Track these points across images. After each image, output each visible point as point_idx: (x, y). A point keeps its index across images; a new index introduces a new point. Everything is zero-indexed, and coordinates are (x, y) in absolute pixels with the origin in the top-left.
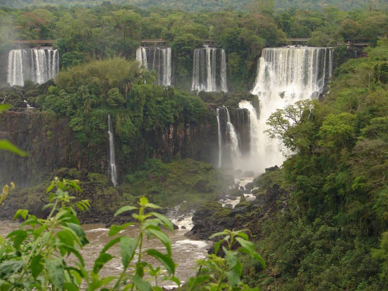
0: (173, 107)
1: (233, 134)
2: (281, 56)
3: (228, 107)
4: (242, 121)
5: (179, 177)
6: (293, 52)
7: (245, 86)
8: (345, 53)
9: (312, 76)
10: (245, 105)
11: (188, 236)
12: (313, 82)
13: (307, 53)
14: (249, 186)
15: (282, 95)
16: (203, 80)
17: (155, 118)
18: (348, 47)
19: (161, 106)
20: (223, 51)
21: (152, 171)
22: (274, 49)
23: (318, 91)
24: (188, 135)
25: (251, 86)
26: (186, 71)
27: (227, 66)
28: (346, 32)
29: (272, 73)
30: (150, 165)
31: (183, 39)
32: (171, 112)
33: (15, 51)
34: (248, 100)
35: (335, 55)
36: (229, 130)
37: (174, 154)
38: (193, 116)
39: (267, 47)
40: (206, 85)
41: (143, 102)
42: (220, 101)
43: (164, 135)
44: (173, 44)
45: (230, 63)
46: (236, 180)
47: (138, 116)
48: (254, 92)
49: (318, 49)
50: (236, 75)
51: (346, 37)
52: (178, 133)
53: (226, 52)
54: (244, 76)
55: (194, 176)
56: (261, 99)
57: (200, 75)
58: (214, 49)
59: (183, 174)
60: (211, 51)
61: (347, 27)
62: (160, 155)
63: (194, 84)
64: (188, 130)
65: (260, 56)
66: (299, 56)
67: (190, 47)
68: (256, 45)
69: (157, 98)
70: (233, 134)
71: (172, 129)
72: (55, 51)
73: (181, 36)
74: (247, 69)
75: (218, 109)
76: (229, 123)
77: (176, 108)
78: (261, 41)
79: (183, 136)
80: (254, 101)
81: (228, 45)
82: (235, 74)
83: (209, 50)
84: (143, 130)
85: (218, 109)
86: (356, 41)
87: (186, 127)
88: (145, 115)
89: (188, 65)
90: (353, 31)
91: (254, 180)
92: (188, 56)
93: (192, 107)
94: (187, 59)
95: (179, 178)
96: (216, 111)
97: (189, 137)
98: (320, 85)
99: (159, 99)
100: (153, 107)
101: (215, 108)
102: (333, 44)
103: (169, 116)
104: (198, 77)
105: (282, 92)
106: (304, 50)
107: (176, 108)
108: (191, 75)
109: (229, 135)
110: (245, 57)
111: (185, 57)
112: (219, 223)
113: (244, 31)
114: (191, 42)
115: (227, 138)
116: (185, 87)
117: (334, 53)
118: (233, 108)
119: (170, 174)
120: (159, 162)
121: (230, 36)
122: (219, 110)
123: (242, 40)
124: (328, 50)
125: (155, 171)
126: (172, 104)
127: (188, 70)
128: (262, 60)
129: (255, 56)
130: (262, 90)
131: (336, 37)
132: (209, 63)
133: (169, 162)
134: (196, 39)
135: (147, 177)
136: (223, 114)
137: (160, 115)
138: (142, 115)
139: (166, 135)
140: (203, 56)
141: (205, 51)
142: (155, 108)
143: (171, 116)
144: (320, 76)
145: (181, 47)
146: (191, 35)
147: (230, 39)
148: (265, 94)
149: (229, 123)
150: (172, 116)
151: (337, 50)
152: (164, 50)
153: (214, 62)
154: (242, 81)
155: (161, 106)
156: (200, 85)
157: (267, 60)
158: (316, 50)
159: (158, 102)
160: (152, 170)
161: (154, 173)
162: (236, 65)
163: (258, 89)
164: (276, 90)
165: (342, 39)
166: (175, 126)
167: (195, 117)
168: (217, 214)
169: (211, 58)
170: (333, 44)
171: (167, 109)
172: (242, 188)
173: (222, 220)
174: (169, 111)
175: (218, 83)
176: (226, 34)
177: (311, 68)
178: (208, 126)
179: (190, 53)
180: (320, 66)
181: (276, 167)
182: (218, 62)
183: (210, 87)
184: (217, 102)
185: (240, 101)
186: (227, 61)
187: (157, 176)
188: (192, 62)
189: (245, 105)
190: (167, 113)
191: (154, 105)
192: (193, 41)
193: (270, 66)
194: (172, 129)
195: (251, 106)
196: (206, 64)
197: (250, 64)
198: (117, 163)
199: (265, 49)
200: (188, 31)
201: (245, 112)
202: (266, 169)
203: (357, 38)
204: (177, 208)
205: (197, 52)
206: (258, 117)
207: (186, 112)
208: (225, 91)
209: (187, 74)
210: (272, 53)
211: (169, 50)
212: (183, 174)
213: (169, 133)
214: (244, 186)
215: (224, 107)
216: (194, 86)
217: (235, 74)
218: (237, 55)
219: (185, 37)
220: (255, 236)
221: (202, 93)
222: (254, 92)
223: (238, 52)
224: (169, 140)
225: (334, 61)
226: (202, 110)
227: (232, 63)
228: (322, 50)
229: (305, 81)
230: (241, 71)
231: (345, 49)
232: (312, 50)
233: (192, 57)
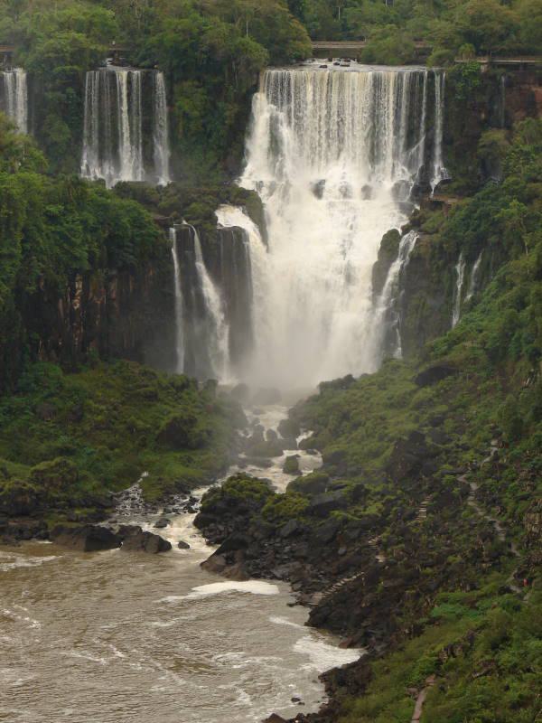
0: (85, 229)
1: (210, 290)
2: (310, 88)
3: (195, 222)
5: (115, 409)
6: (341, 78)
7: (219, 166)
8: (477, 82)
9: (389, 138)
10: (231, 217)
11: (214, 568)
12: (395, 155)
13: (377, 83)
14: (290, 429)
15: (318, 191)
16: (109, 151)
17: (45, 258)
18: (483, 68)
19: (59, 228)
20: (160, 76)
21: (46, 397)
22: (293, 73)
23: (407, 177)
24: (114, 300)
25: (238, 169)
26: (66, 128)
27: (171, 117)
28: (478, 29)
29: (286, 132)
30: (37, 381)
31: (59, 47)
32: (83, 243)
34: (235, 204)
35: (449, 89)
36: (197, 282)
37: (84, 350)
38: (126, 252)
39: (273, 64)
40: (117, 164)
41: (22, 219)
42: (172, 207)
43: (61, 301)
44: (30, 59)
45: (180, 108)
47: (11, 256)
48: (246, 182)
49: (407, 71)
50: (194, 139)
51: (477, 39)
52: (91, 294)
53: (170, 80)
54: (217, 139)
55: (150, 406)
56: (270, 203)
57: (101, 137)
58: (136, 72)
59: (123, 403)
60: (129, 76)
61: (478, 18)
62: (53, 353)
63: (85, 161)
64: (113, 286)
65: (255, 89)
66: (353, 87)
67: (75, 67)
68: (249, 63)
69: (47, 208)
70: (210, 290)
71: (79, 285)
73: (50, 37)
74: (224, 124)
75: (173, 230)
76: (200, 265)
77: (94, 230)
78: (262, 53)
79: (102, 303)
80: (248, 201)
81: (175, 62)
82: (192, 135)
83: (123, 74)
84: (18, 291)
85: (173, 230)
86: (502, 53)
87: (110, 279)
88: (24, 251)
89: (72, 112)
90: (497, 27)
91: (292, 413)
92: (70, 90)
93: (127, 227)
94: (68, 98)
95: (115, 413)
96: (168, 235)
97: (116, 304)
98: (410, 164)
99: (53, 209)
100: (40, 230)
101: (166, 226)
102: (440, 61)
103: (78, 252)
104: (95, 142)
105: (315, 177)
106: (370, 73)
107: (94, 230)
108: (78, 138)
109: (200, 299)
110: (217, 91)
111: (63, 93)
112: (285, 532)
113: (217, 30)
114: (78, 55)
115: (197, 305)
116: (64, 169)
117: (446, 82)
118: (208, 226)
119: (91, 402)
120: (56, 370)
121: (181, 39)
122: (177, 233)
123: (212, 48)
124: (431, 75)
125: (51, 395)
126: (84, 222)
127: (71, 126)
129: (244, 90)
130: (266, 178)
131: (447, 43)
132: (125, 108)
133: (77, 371)
134: (93, 47)
135: (34, 411)
136: (184, 240)
137: (57, 250)
138: (18, 252)
139: (65, 302)
140: (107, 90)
141: (113, 76)
142: (47, 235)
143: (82, 252)
144: (409, 145)
145: (52, 67)
146: (81, 37)
147: (184, 46)
148: (272, 189)
149: (200, 265)
150: (86, 254)
151: (456, 76)
152: (8, 76)
153: (137, 103)
154: (211, 154)
155: (59, 228)
156: (101, 165)
157: (274, 101)
158: (400, 76)
159: (52, 219)
160: (46, 393)
161: (50, 399)
162: (196, 113)
163: (253, 174)
164: (301, 179)
165: (467, 47)
166: (86, 278)
167: (132, 254)
168: (271, 510)
169: (129, 95)
170: (440, 61)
171: (74, 236)
172: (271, 433)
173: (291, 525)
174: (79, 241)
175: (149, 161)
176: (171, 36)
177: (389, 121)
178: (151, 273)
179: (76, 81)
180: (412, 117)
181: (349, 378)
182: (148, 106)
184: (163, 211)
185: (217, 207)
186: (170, 103)
187: (60, 410)
188: (80, 105)
189: (231, 217)
190: (73, 245)
191: (44, 226)
192: (82, 51)
193: (282, 116)
194: (79, 285)
195: (247, 219)
196: (115, 111)
197: (230, 110)
199: (268, 71)
200: (64, 26)
201: (238, 234)
202: (324, 386)
203: (506, 45)
204: (134, 491)
205: (92, 80)
207: (114, 242)
209: (69, 136)
210: (285, 84)
211: (21, 75)
212: (123, 403)
213: (73, 297)
214: (274, 428)
215: (184, 222)
216: (87, 166)
217: (192, 135)
218: (197, 87)
219: (64, 39)
220: (429, 570)
221: (123, 189)
222: (246, 182)
223: (198, 79)
224: (72, 314)
225: (446, 100)
226: (150, 235)
227: (186, 108)
228: (415, 74)
229: (374, 155)
230: (209, 127)
231: (475, 74)
232: (389, 73)
233: (80, 94)
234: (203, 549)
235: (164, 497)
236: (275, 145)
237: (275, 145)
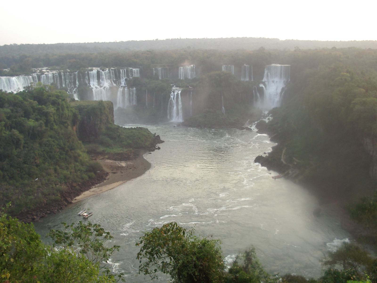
1: (258, 94)
4: (261, 91)
11: (258, 132)
14: (269, 114)
25: (262, 78)
29: (269, 74)
33: (181, 67)
34: (262, 83)
46: (263, 112)
48: (263, 81)
56: (266, 83)
70: (258, 94)
72: (194, 67)
80: (264, 83)
91: (269, 112)
128: (265, 69)
148: (267, 81)
163: (265, 79)
172: (266, 115)
175: (250, 78)
183: (247, 79)
189: (261, 85)
198: (224, 107)
202: (273, 108)
206: (266, 89)
208: (252, 80)
214: (266, 114)
222: (263, 81)
234: (256, 130)
235: (251, 123)
236: (268, 75)
237: (268, 75)
